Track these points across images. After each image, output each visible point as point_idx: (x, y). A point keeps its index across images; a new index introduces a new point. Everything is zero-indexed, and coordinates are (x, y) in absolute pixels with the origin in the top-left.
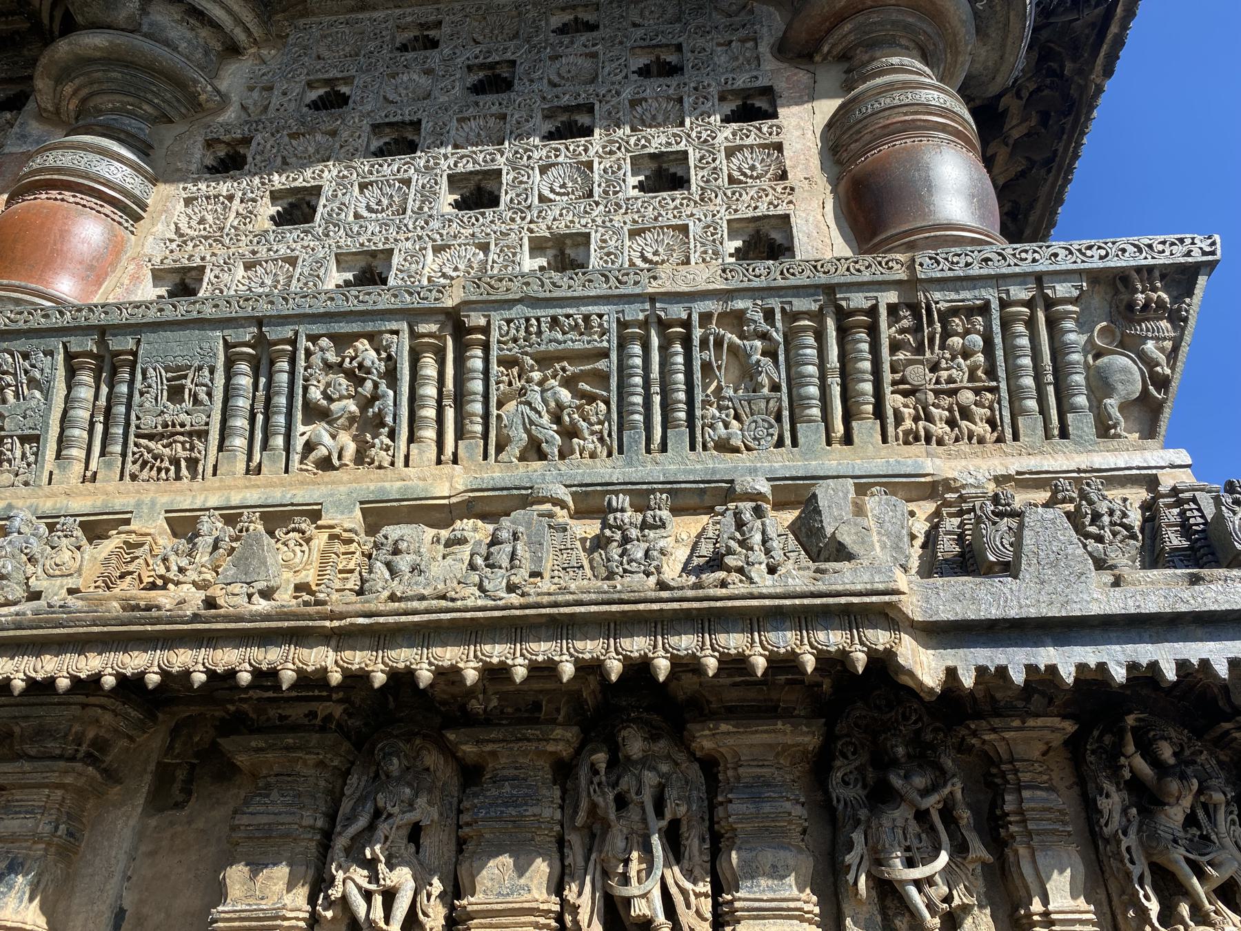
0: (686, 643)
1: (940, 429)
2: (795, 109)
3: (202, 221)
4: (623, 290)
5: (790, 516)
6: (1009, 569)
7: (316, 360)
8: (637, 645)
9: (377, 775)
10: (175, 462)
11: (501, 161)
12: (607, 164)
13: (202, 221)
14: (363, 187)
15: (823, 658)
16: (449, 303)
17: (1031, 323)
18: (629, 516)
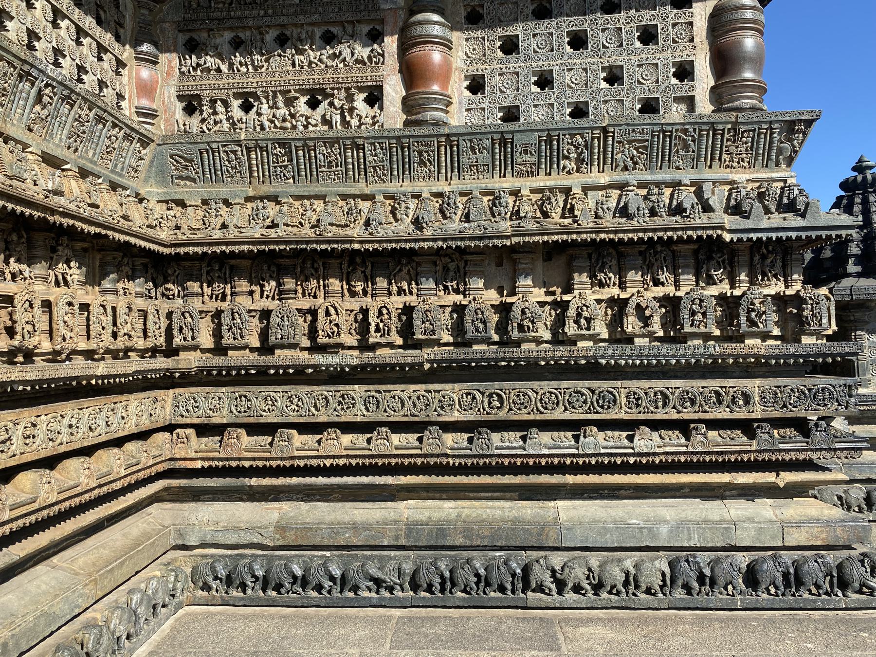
0: (680, 233)
1: (735, 164)
2: (699, 4)
3: (474, 50)
4: (655, 122)
5: (693, 189)
6: (748, 217)
7: (565, 141)
8: (670, 234)
9: (599, 255)
10: (527, 172)
11: (586, 26)
12: (627, 29)
13: (474, 50)
14: (534, 35)
15: (708, 236)
16: (604, 125)
17: (765, 135)
18: (656, 191)
